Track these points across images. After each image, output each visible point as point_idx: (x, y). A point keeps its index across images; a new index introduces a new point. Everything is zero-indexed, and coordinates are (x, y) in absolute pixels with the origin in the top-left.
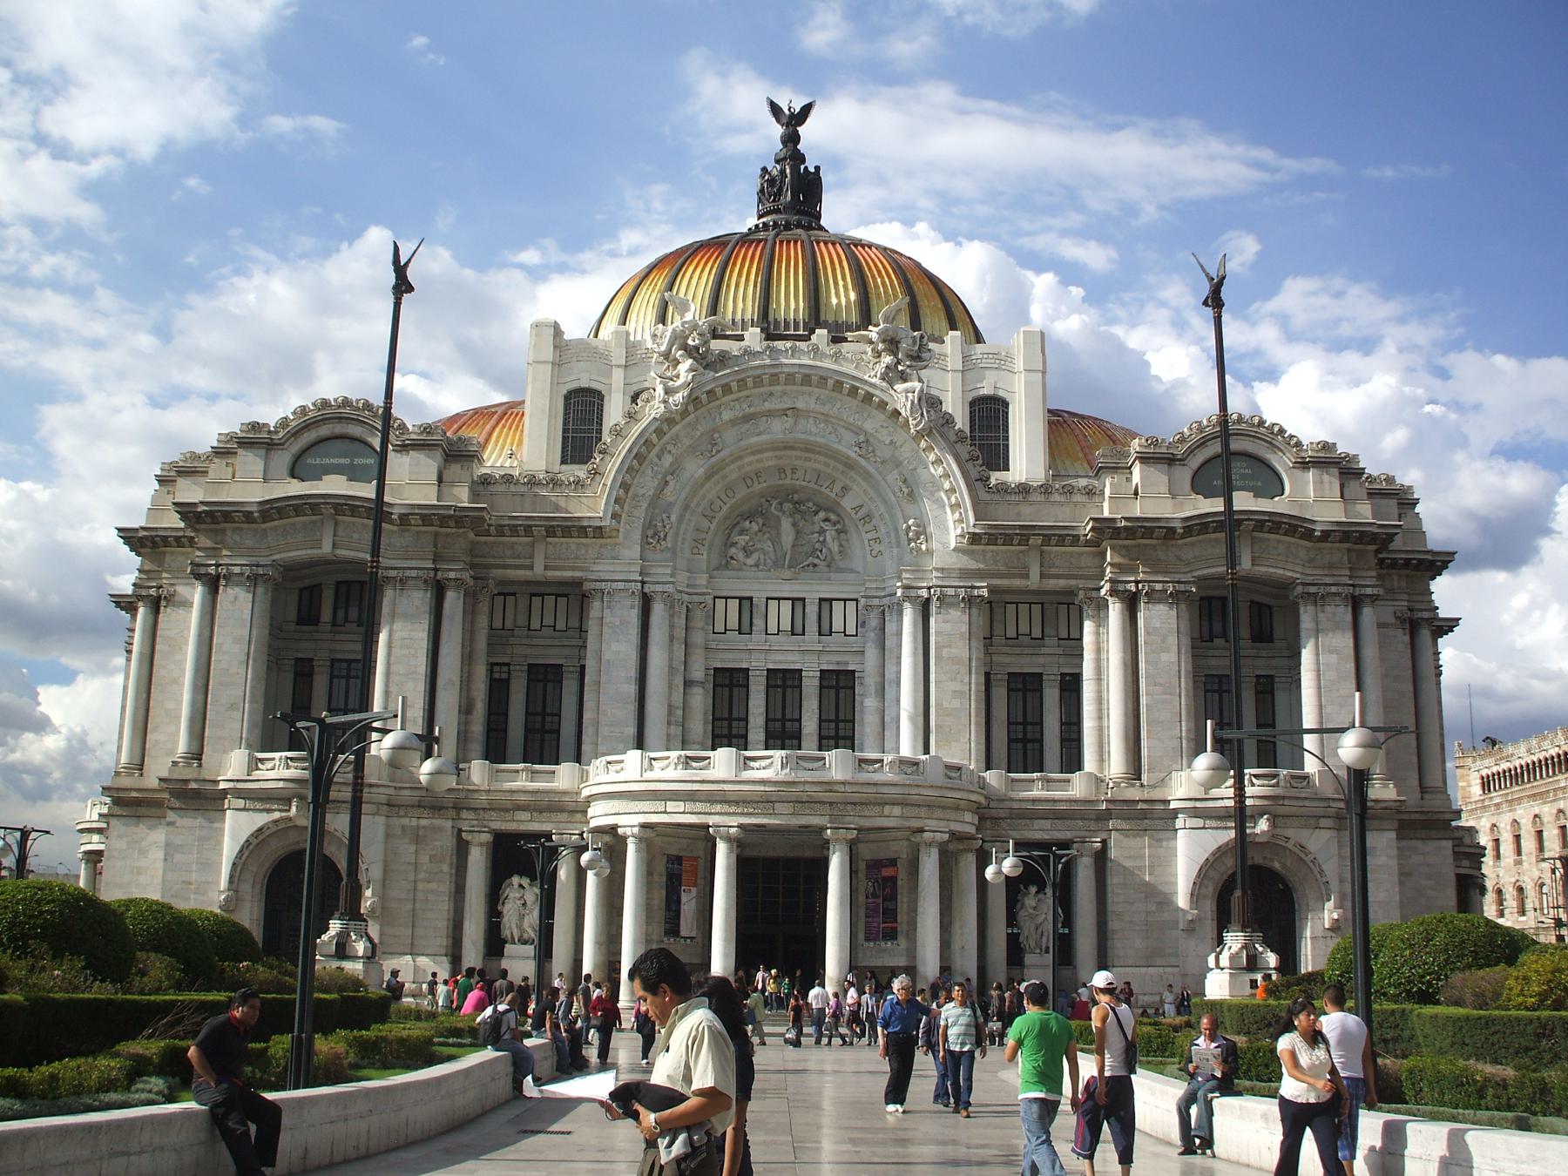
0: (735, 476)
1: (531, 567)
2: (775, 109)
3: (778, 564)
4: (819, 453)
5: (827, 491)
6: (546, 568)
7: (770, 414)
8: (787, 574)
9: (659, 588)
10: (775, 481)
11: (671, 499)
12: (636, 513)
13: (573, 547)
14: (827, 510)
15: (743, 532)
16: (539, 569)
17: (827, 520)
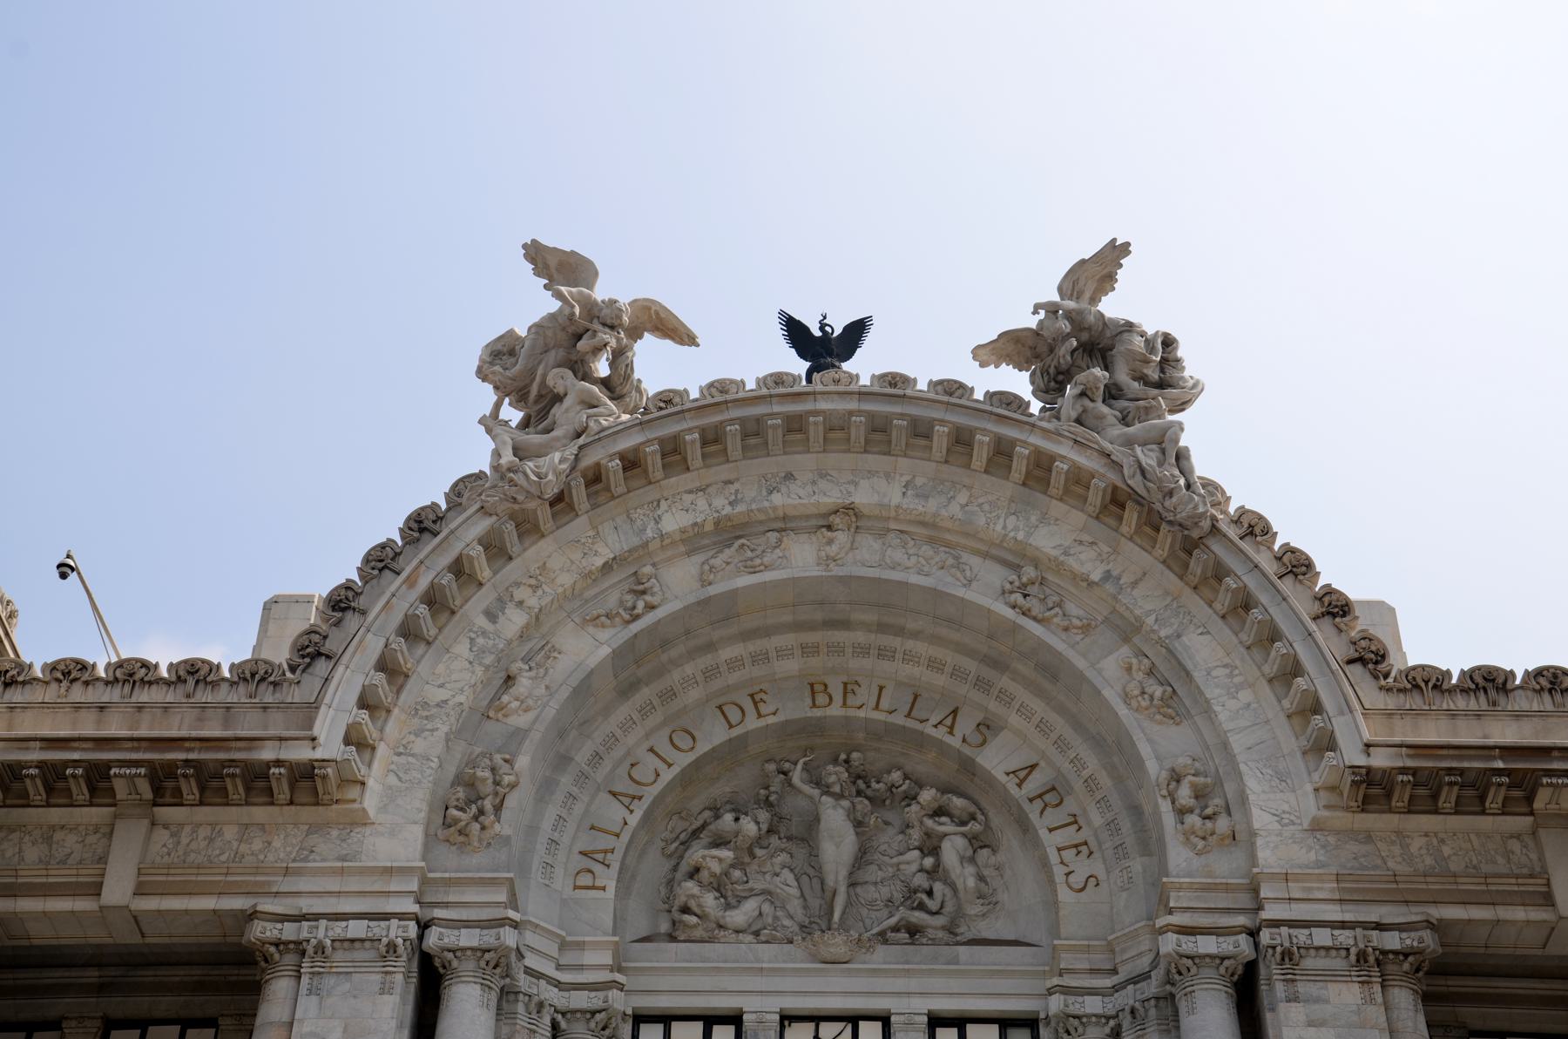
0: (694, 694)
1: (96, 890)
2: (795, 332)
3: (817, 923)
4: (916, 635)
5: (940, 733)
6: (141, 890)
7: (785, 524)
8: (836, 944)
9: (468, 938)
10: (796, 709)
11: (521, 720)
12: (419, 746)
13: (230, 833)
14: (945, 790)
15: (719, 842)
16: (118, 890)
17: (939, 812)
